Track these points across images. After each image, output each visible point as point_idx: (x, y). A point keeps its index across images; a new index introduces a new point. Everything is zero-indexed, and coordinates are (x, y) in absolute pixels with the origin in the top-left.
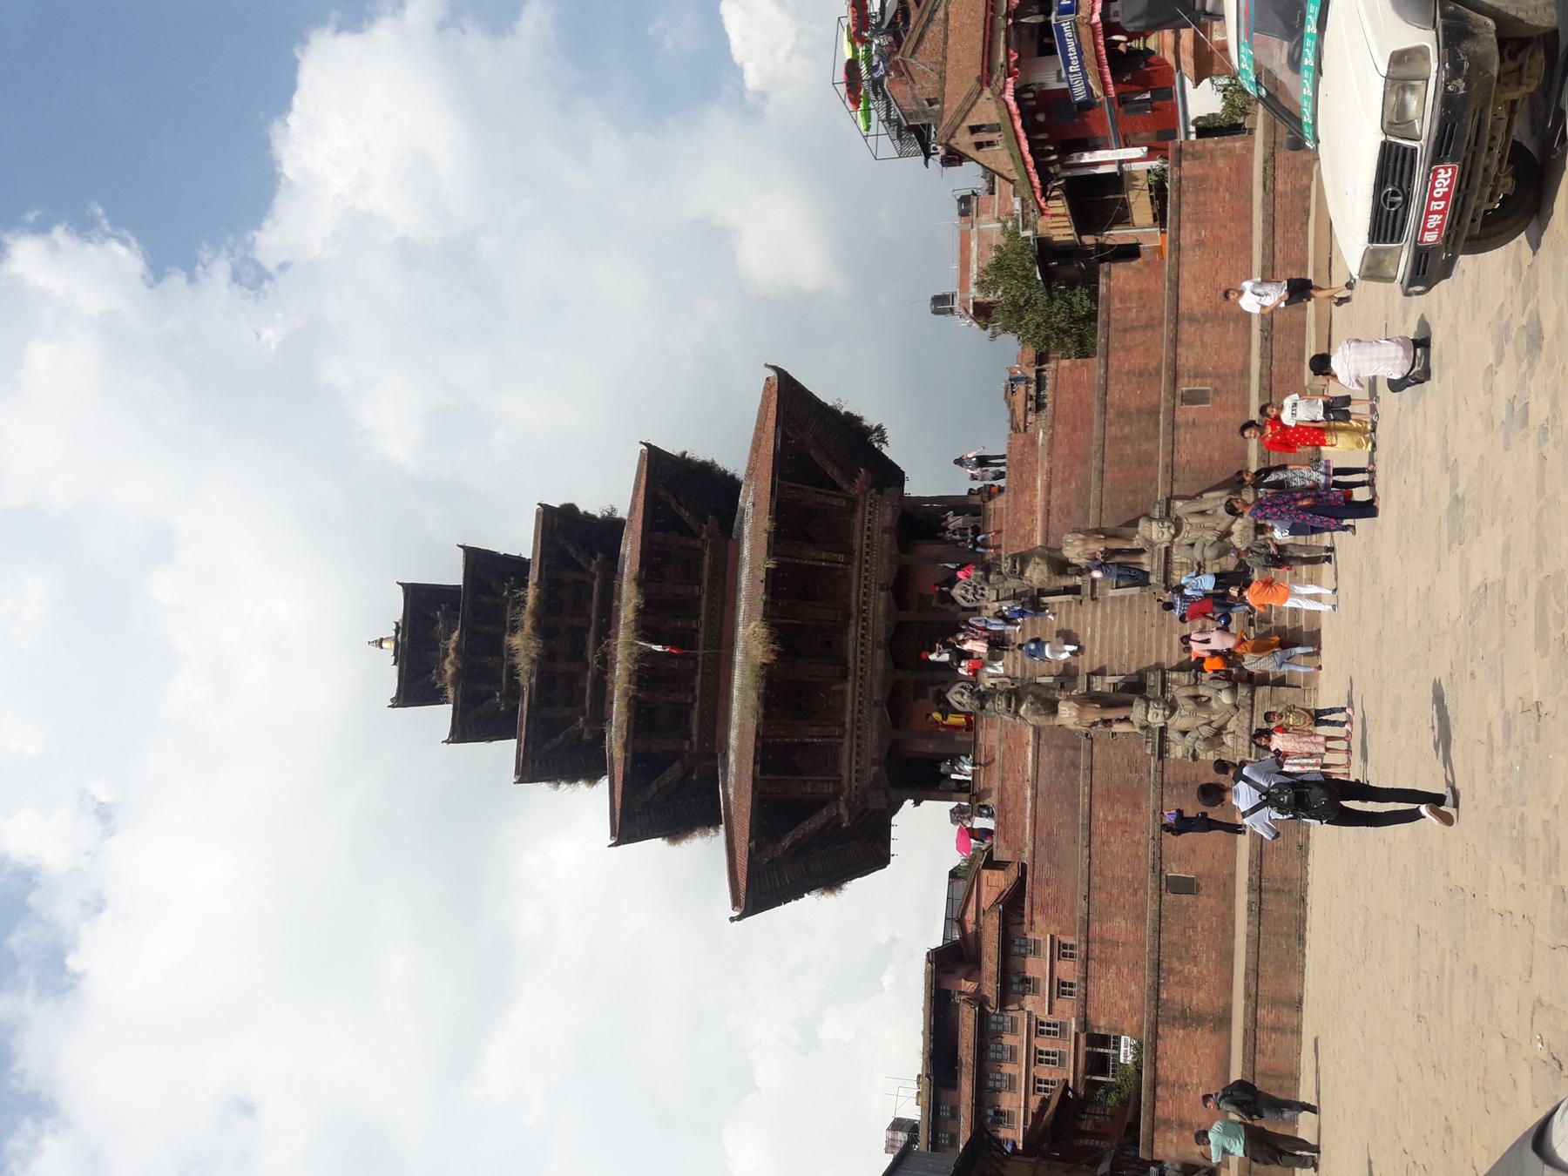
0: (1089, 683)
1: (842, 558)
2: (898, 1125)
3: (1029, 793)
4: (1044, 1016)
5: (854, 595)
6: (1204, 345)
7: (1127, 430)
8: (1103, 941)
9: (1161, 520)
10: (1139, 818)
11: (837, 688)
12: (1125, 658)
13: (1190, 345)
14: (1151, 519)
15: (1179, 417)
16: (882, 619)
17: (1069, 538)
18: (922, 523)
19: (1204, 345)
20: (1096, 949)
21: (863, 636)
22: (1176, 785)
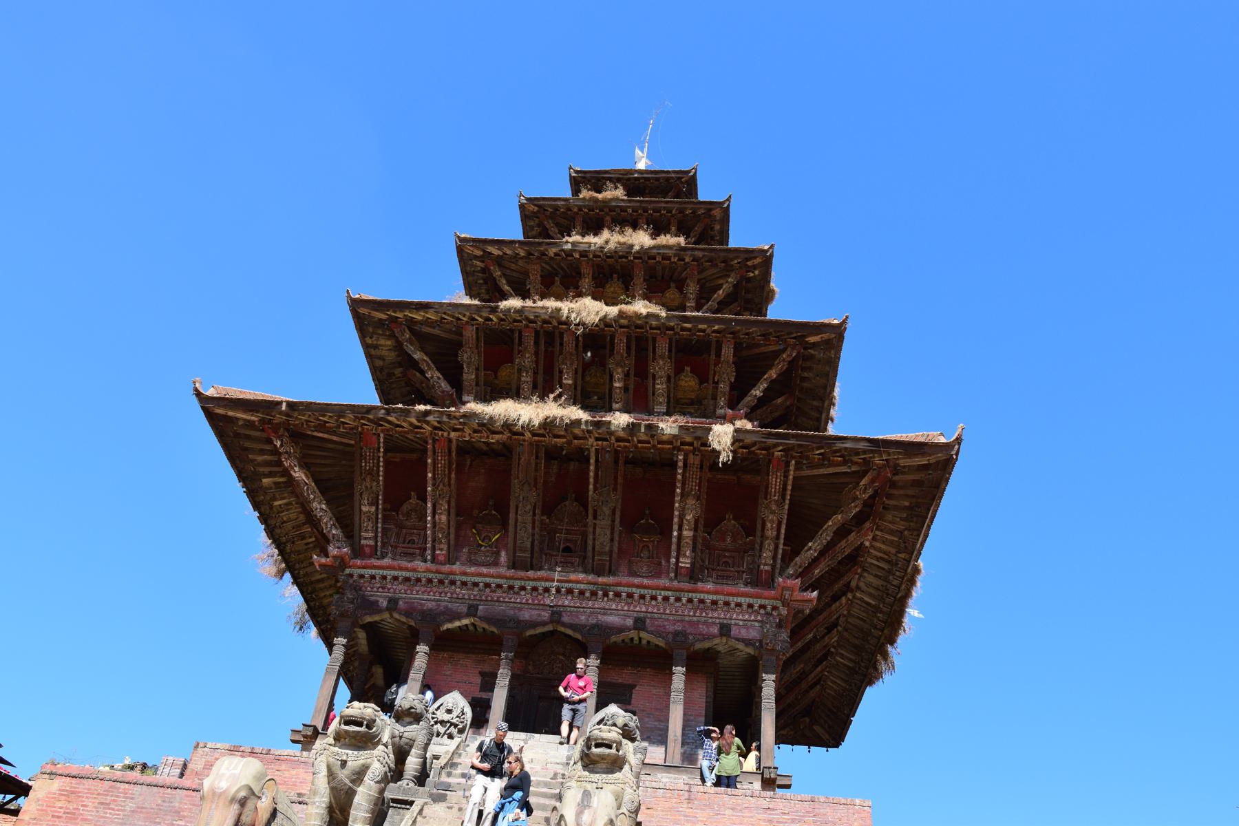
1: (685, 563)
5: (631, 579)
16: (593, 621)
21: (570, 591)
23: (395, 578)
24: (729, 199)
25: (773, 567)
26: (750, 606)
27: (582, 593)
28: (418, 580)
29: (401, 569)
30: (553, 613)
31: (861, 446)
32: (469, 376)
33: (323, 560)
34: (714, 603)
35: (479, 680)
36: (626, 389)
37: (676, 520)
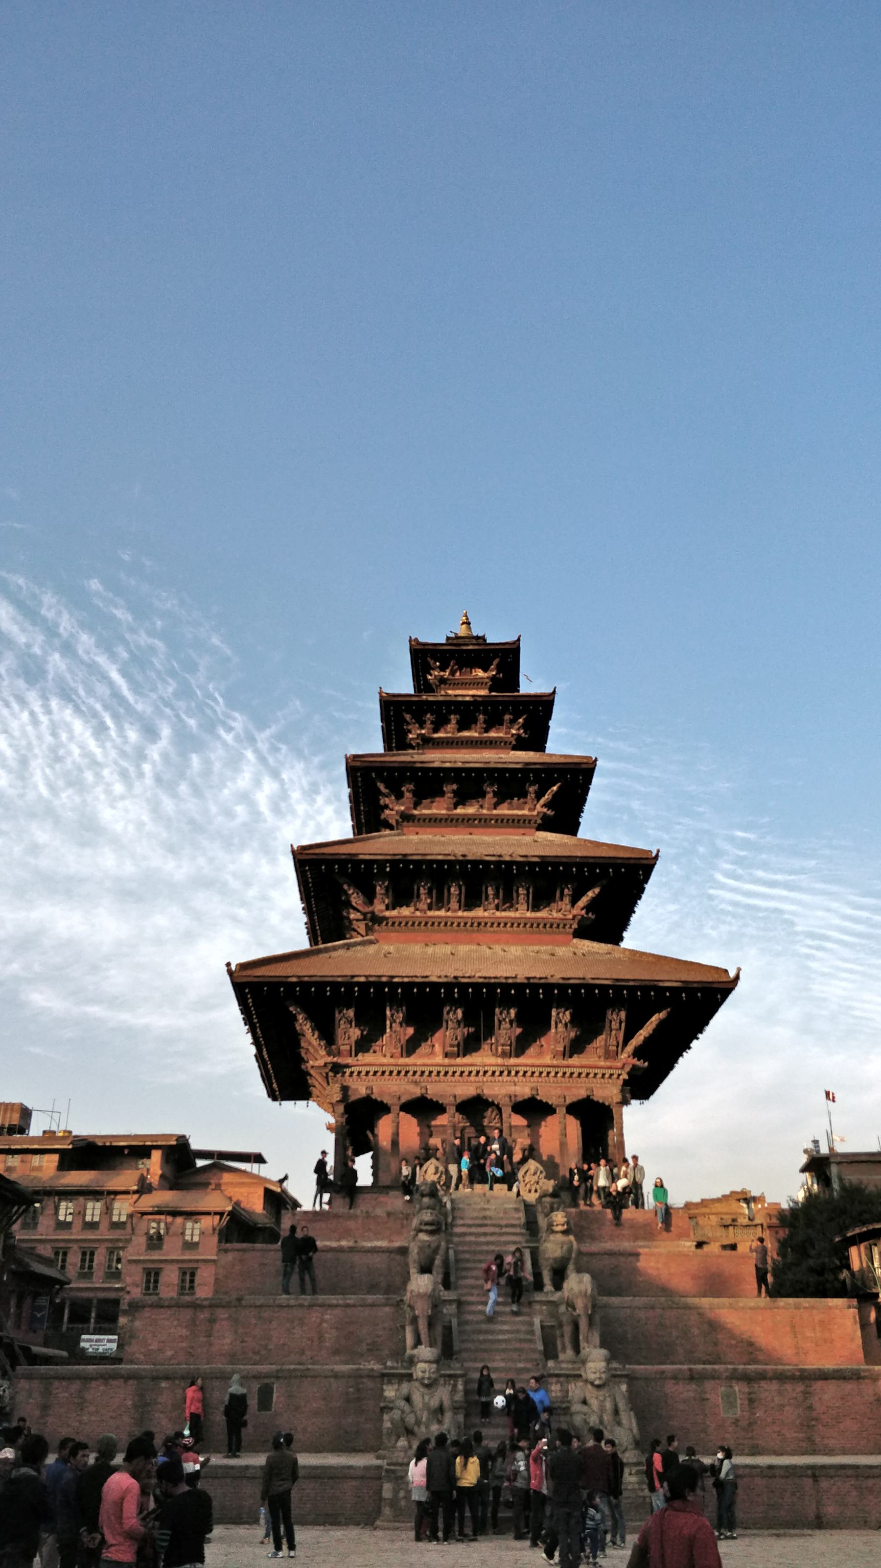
0: (450, 1302)
2: (26, 1113)
3: (344, 1243)
4: (128, 1254)
6: (782, 1407)
7: (696, 1331)
8: (212, 1321)
9: (608, 1369)
12: (475, 1337)
13: (779, 1392)
14: (608, 1361)
15: (709, 1385)
16: (503, 1091)
17: (587, 1278)
18: (597, 1124)
19: (782, 1407)
20: (203, 1315)
22: (358, 1390)
25: (617, 1047)
37: (553, 1023)
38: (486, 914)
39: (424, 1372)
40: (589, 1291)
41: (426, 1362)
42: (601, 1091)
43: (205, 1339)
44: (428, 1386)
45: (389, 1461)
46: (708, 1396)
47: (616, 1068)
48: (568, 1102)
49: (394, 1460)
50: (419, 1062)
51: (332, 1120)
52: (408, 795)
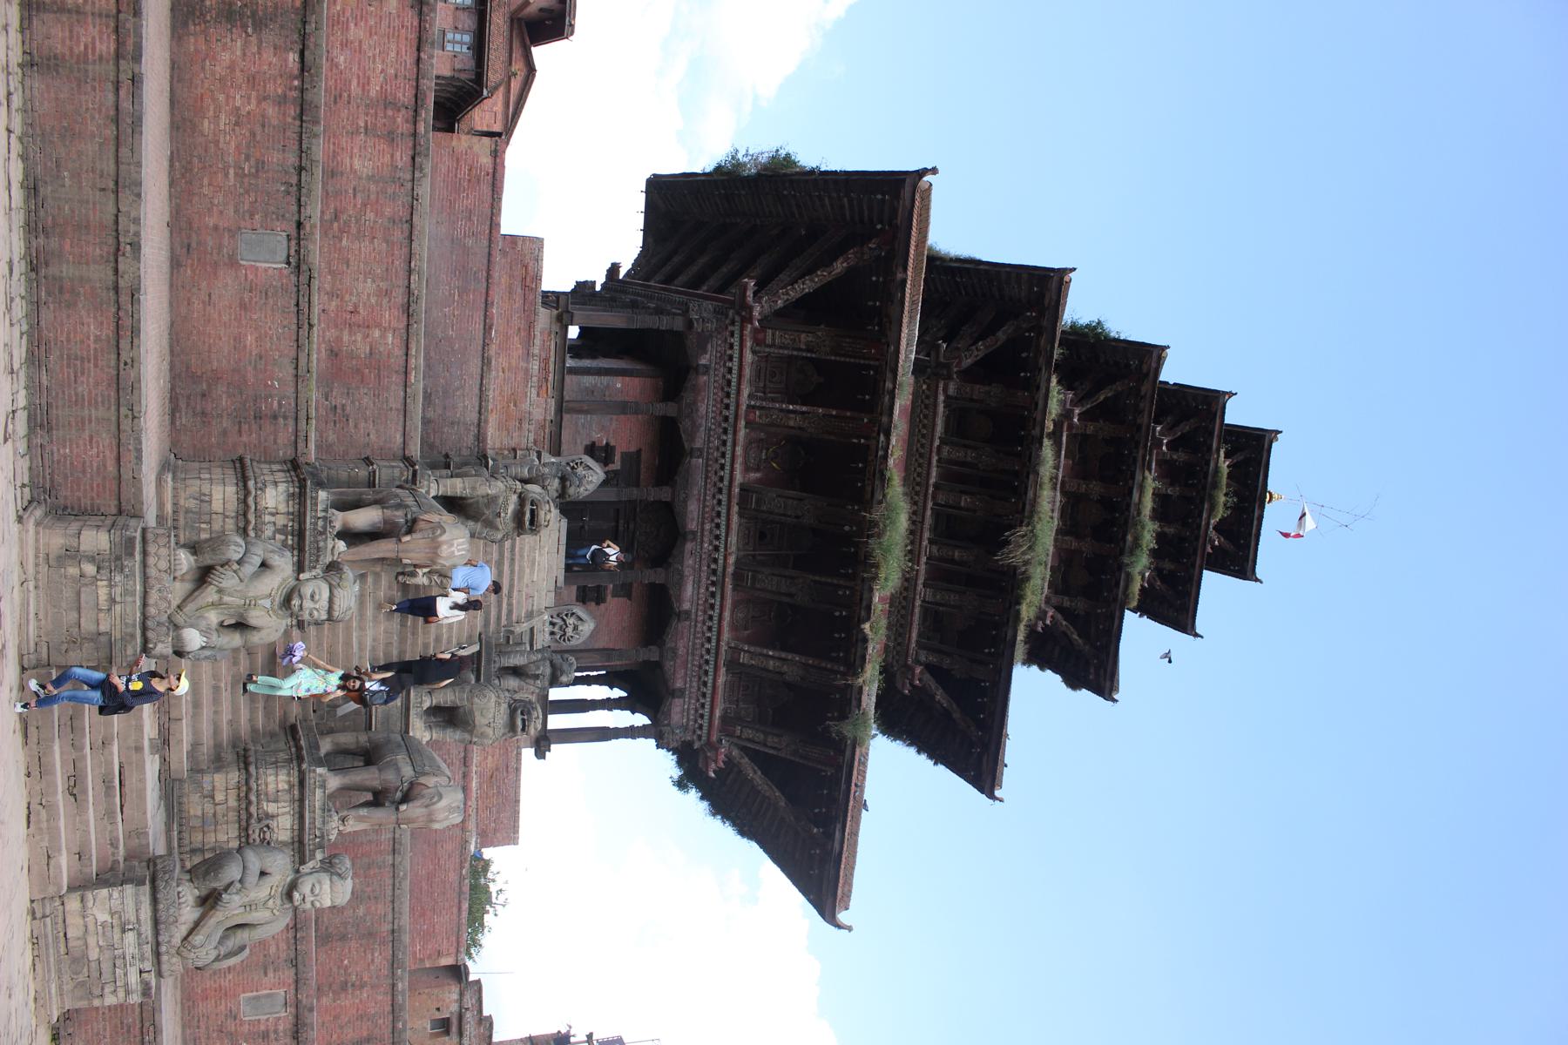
10: (331, 334)
11: (754, 476)
16: (687, 571)
20: (401, 122)
21: (716, 549)
23: (730, 370)
24: (1196, 635)
26: (702, 716)
27: (715, 561)
28: (728, 395)
29: (740, 376)
30: (694, 533)
31: (837, 845)
32: (978, 391)
33: (750, 293)
34: (705, 684)
35: (633, 449)
36: (953, 561)
37: (783, 655)
38: (925, 543)
39: (312, 596)
40: (436, 826)
41: (331, 601)
42: (678, 709)
43: (362, 124)
44: (287, 602)
45: (150, 536)
46: (271, 975)
47: (709, 734)
48: (668, 664)
49: (152, 549)
50: (739, 450)
51: (622, 273)
52: (1091, 429)
